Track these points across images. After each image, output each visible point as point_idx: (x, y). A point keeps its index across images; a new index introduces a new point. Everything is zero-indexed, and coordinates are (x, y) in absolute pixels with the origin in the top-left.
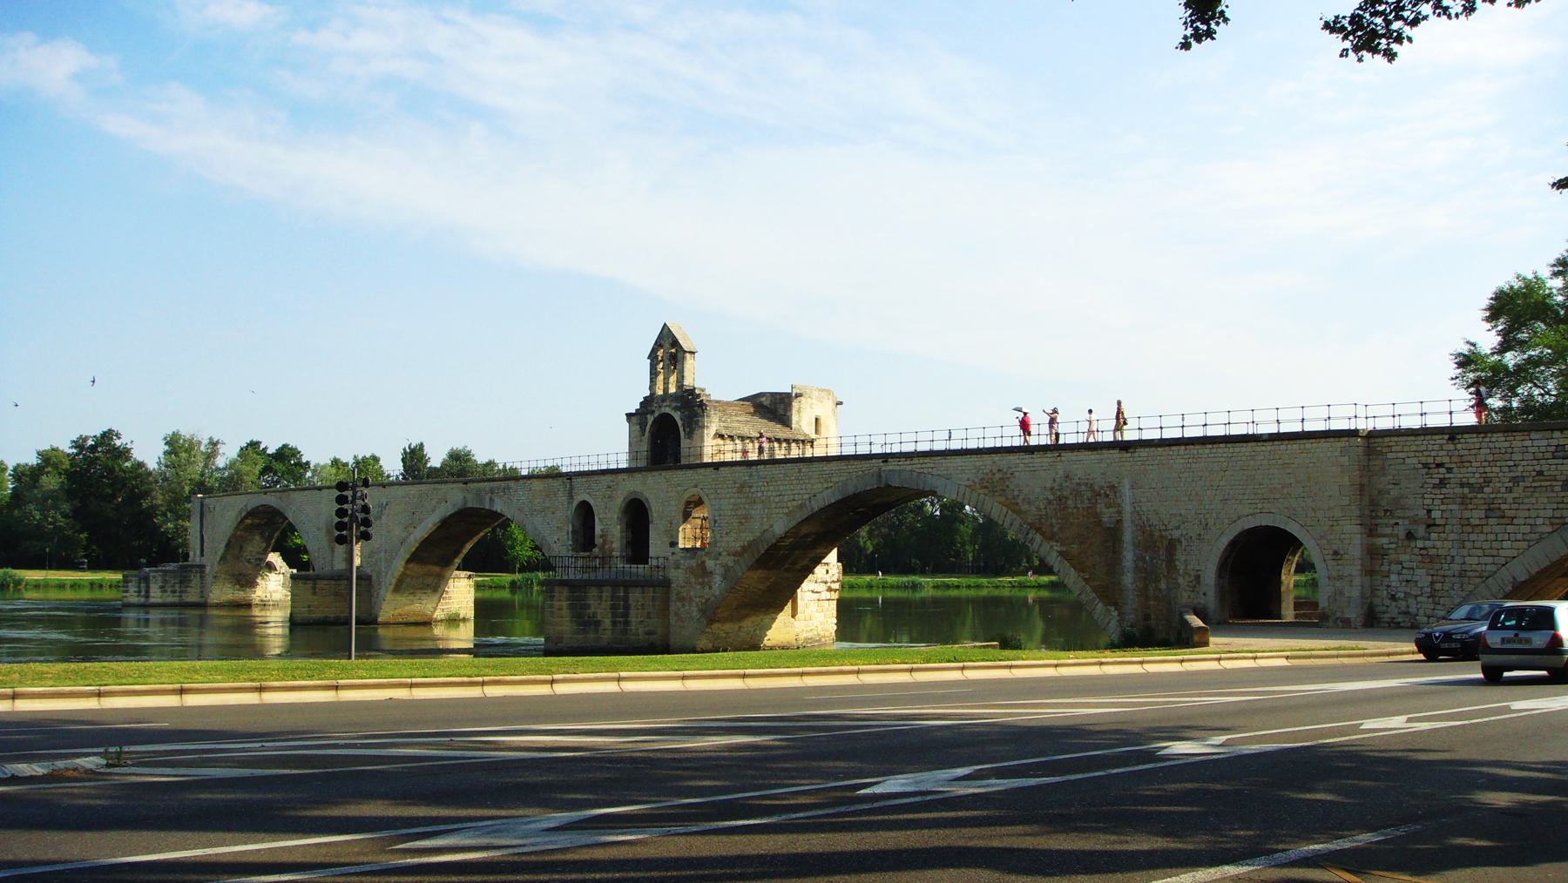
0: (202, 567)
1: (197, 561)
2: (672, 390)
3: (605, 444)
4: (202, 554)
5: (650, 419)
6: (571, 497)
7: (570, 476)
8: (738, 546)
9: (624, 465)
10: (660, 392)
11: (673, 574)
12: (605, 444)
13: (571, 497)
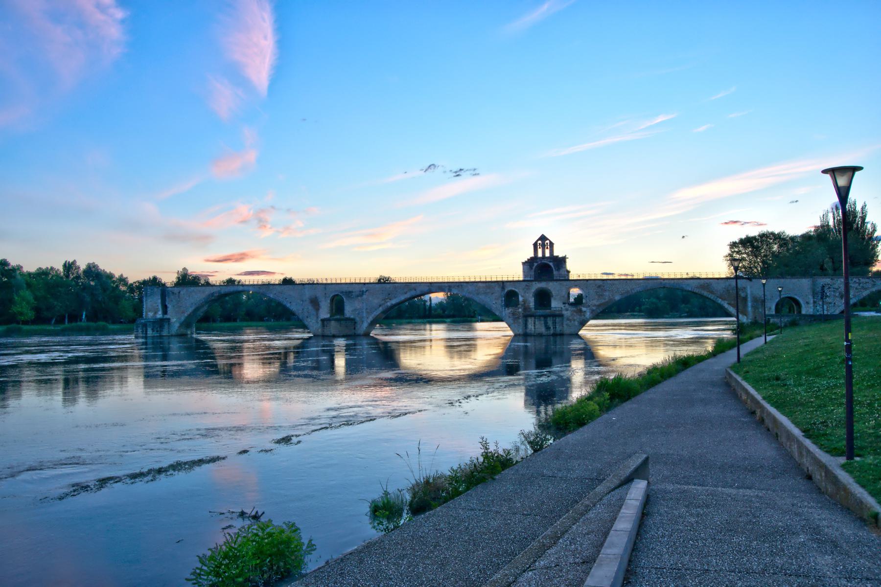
0: (169, 319)
1: (159, 315)
2: (547, 254)
3: (515, 272)
4: (165, 312)
5: (536, 264)
6: (503, 288)
7: (503, 282)
8: (597, 303)
9: (521, 279)
10: (540, 255)
11: (564, 312)
12: (515, 272)
13: (503, 288)
